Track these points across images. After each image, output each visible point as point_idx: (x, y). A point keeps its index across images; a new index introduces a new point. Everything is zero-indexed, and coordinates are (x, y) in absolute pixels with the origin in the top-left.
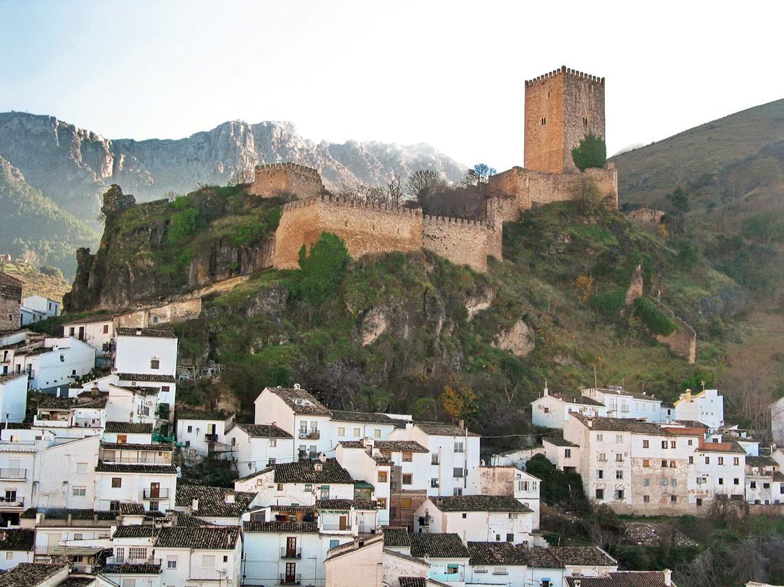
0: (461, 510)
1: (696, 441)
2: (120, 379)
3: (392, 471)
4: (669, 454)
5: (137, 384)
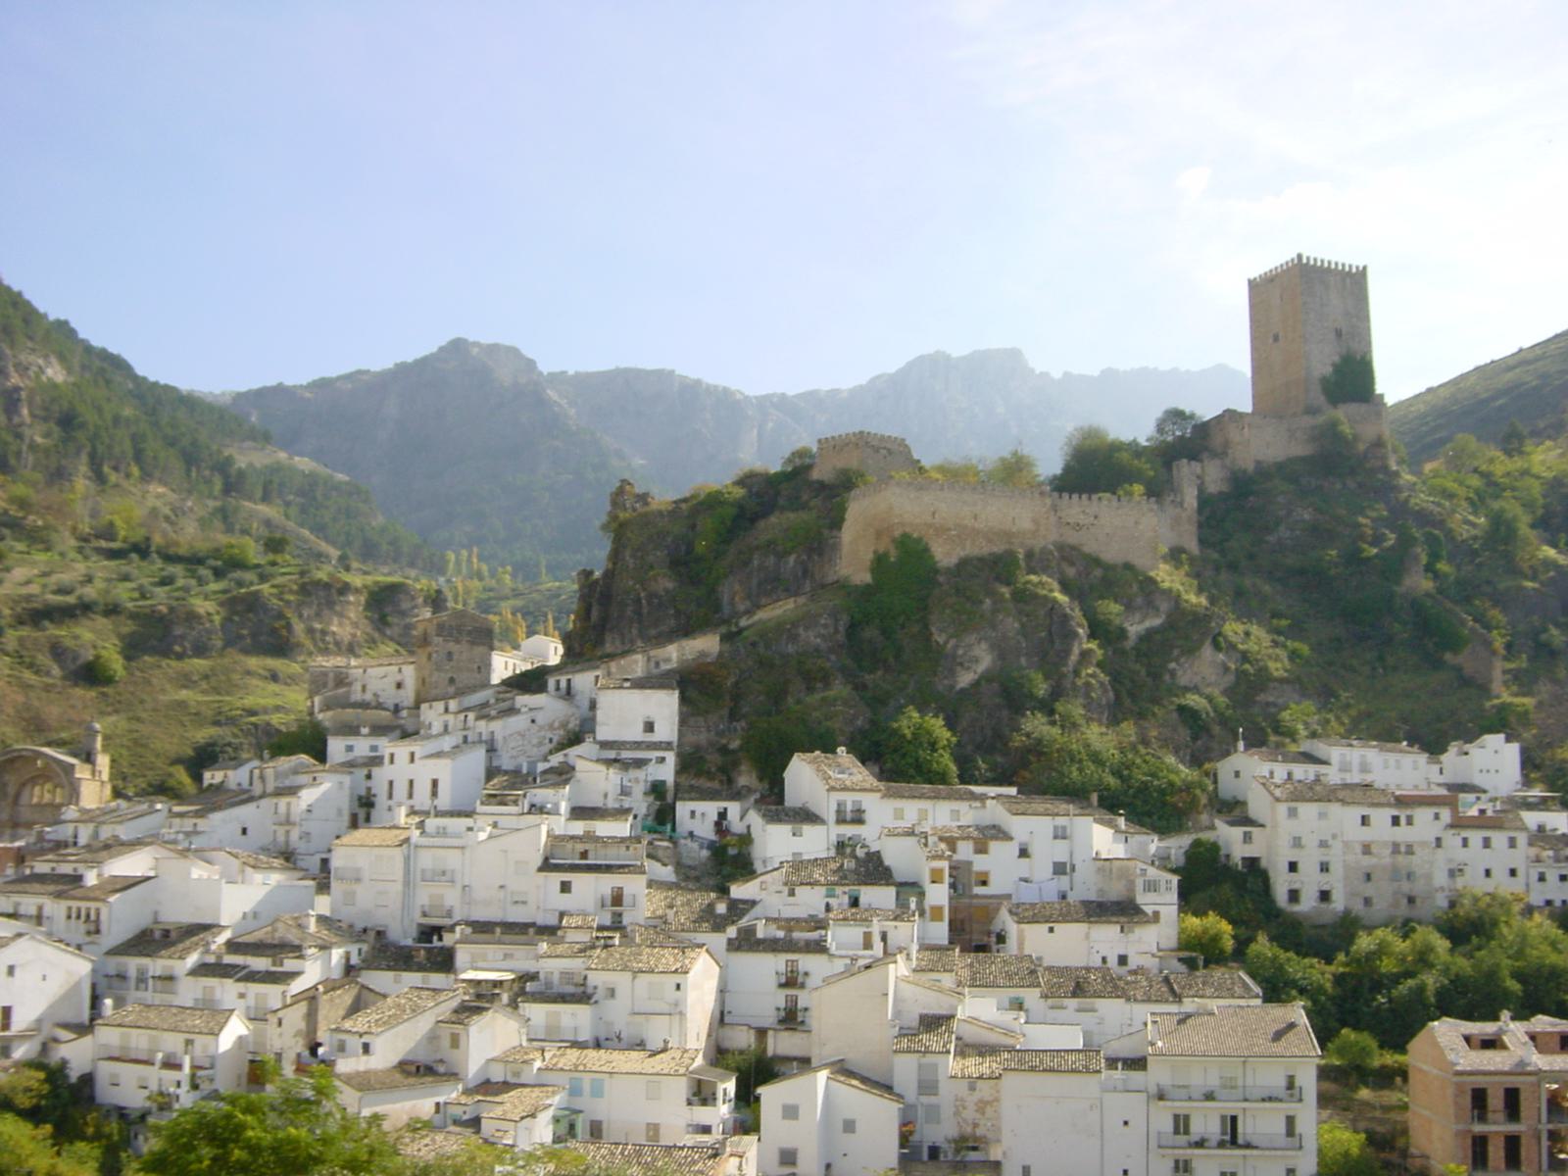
0: (1046, 922)
1: (1446, 815)
2: (601, 747)
3: (951, 868)
4: (1403, 833)
5: (620, 756)
